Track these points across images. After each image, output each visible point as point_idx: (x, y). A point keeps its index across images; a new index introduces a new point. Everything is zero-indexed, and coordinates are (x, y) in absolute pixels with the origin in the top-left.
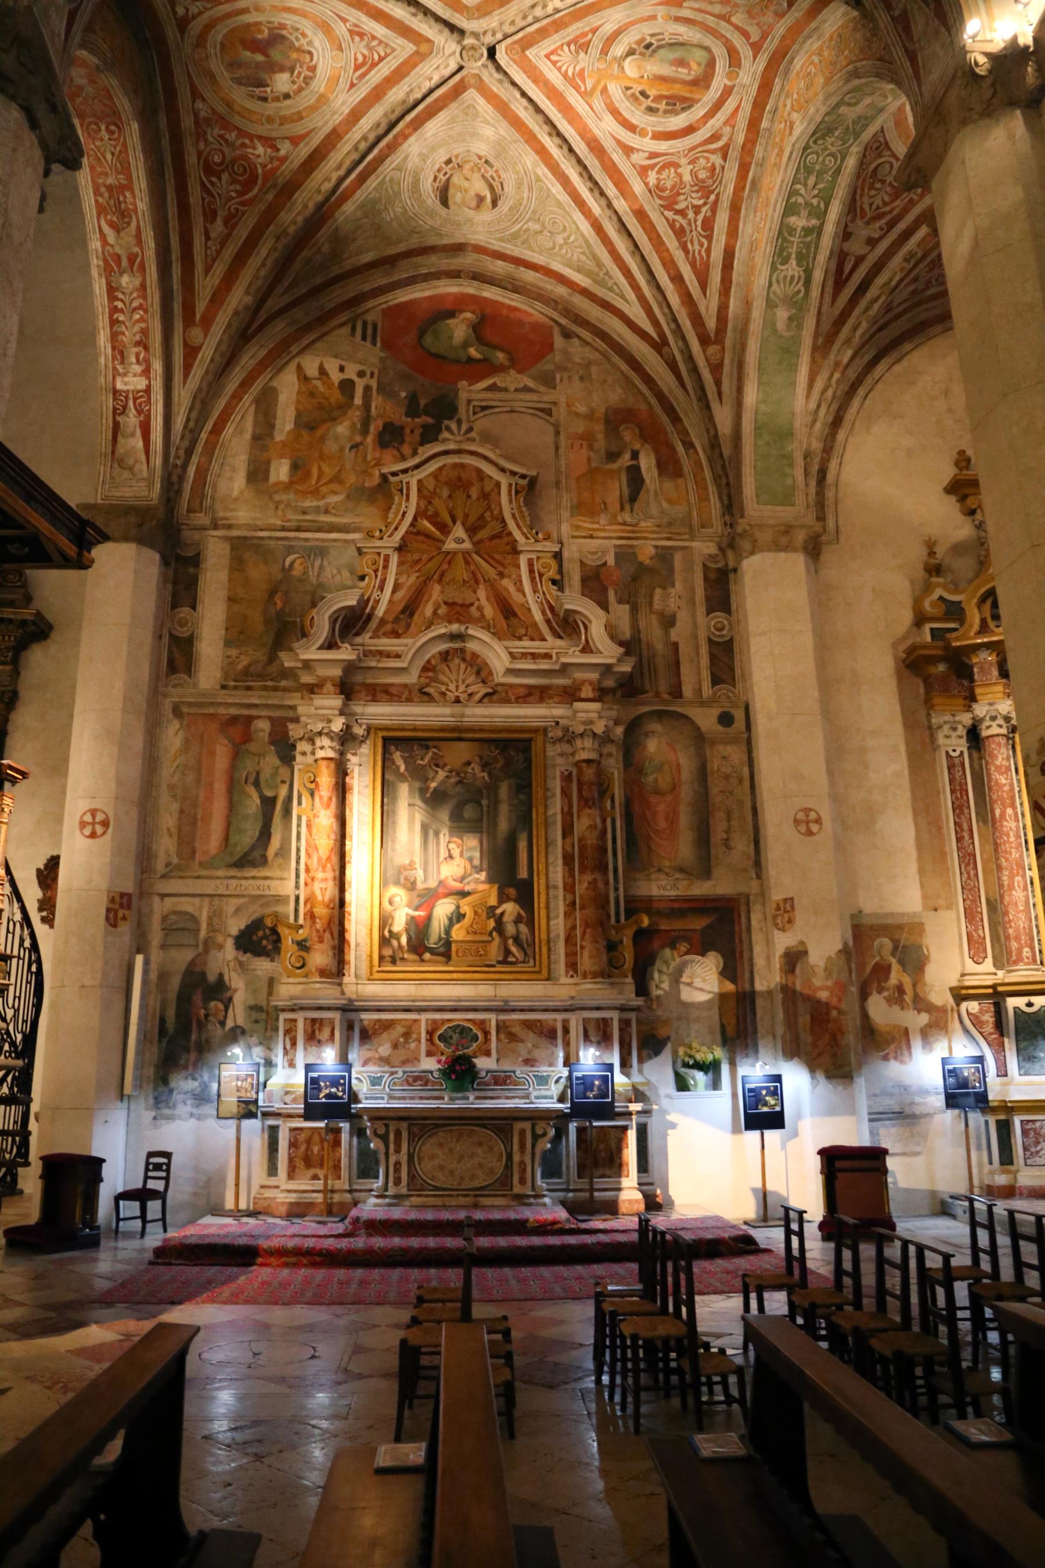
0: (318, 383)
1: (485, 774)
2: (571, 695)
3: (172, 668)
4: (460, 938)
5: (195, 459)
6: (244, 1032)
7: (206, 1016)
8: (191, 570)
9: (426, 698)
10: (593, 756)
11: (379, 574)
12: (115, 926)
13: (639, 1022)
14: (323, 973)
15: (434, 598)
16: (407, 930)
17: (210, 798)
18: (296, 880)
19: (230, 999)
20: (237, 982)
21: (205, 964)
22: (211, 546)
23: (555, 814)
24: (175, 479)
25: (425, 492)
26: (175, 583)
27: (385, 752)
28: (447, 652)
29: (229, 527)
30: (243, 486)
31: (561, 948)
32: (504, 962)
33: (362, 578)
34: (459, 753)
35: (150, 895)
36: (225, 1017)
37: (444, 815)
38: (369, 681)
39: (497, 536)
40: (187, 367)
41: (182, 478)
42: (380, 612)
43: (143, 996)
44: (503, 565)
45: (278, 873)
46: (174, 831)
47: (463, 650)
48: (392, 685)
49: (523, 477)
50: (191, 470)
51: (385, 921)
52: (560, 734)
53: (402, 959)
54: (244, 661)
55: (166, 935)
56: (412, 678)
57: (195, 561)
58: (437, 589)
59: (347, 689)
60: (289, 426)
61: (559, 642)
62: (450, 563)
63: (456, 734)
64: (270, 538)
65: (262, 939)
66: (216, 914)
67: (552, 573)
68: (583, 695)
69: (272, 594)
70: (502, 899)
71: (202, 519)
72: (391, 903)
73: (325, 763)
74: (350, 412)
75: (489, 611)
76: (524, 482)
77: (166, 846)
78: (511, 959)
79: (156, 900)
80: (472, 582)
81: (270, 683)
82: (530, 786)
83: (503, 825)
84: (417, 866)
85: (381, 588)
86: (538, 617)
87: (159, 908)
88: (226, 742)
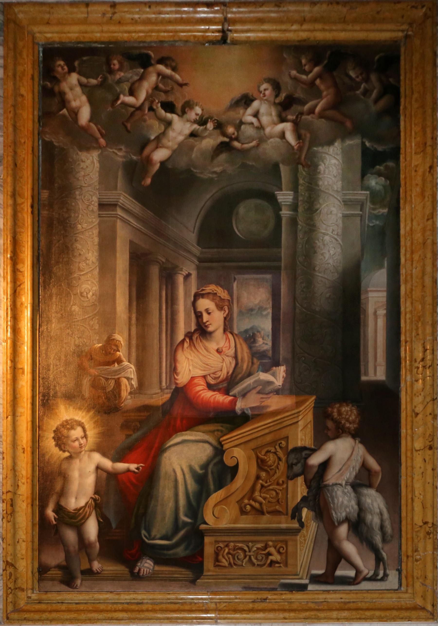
4: (224, 524)
16: (98, 505)
32: (328, 578)
53: (89, 573)
78: (343, 571)
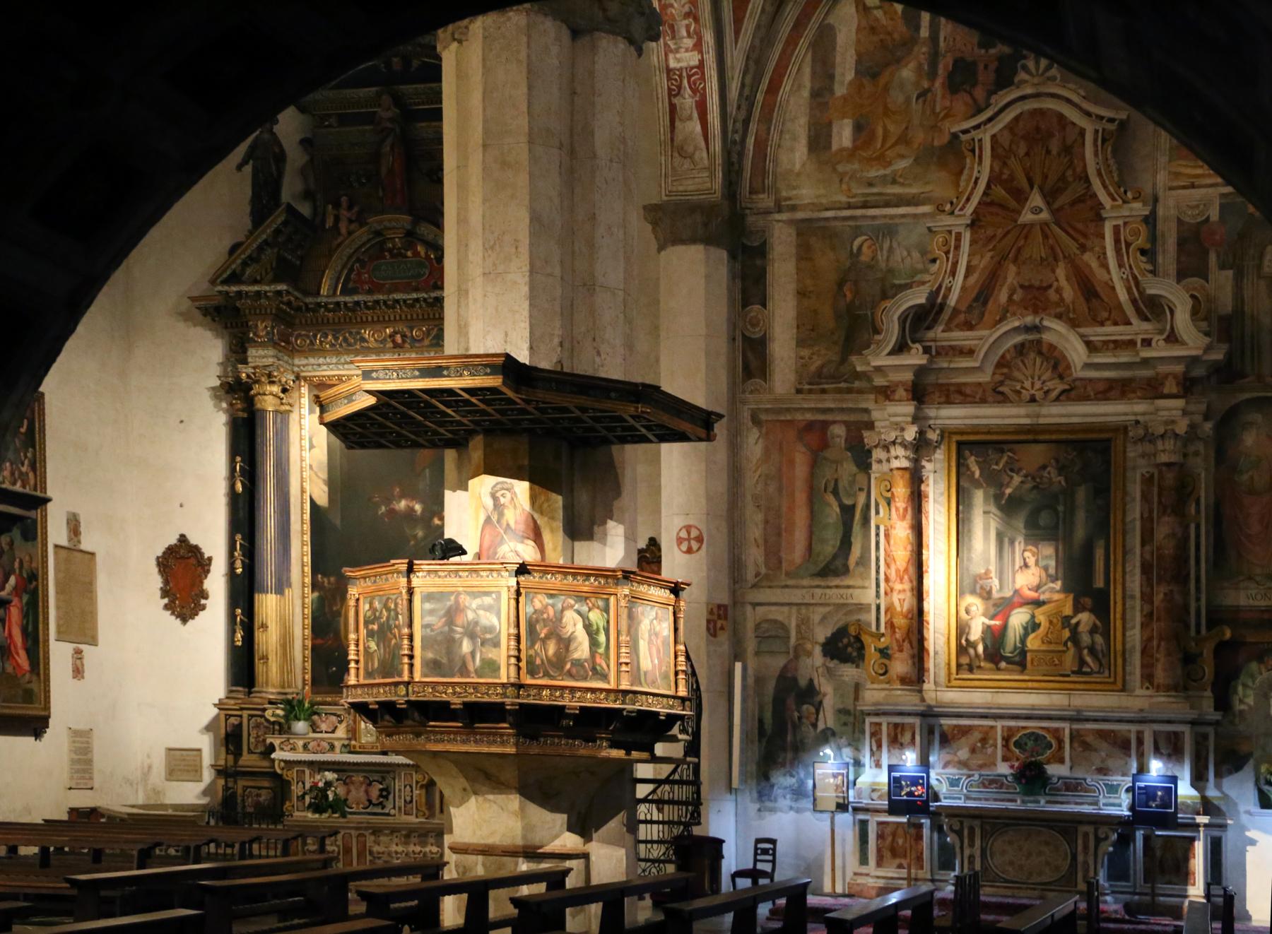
0: (878, 14)
1: (1061, 479)
2: (1153, 389)
3: (748, 373)
4: (1035, 648)
5: (753, 127)
6: (834, 734)
7: (800, 718)
8: (758, 262)
9: (1000, 398)
10: (1174, 458)
11: (951, 256)
12: (715, 635)
13: (1216, 734)
14: (904, 680)
15: (1009, 280)
16: (983, 639)
17: (791, 509)
18: (877, 590)
19: (821, 703)
20: (826, 687)
21: (796, 670)
22: (776, 233)
23: (1134, 519)
24: (735, 158)
25: (1000, 150)
26: (744, 278)
27: (960, 456)
28: (1022, 345)
29: (793, 208)
30: (805, 158)
31: (1136, 659)
32: (1079, 672)
33: (934, 261)
34: (1035, 455)
35: (743, 604)
36: (817, 719)
37: (1020, 523)
38: (940, 381)
39: (1080, 200)
40: (738, 22)
41: (741, 154)
42: (952, 300)
43: (744, 700)
44: (1085, 236)
45: (859, 582)
46: (761, 541)
47: (1039, 342)
48: (965, 384)
49: (1111, 120)
50: (750, 141)
51: (962, 629)
52: (1141, 432)
53: (979, 667)
54: (818, 362)
55: (760, 643)
56: (985, 377)
57: (761, 251)
58: (1012, 269)
59: (919, 392)
60: (850, 76)
61: (1146, 326)
62: (1026, 238)
63: (1032, 434)
64: (835, 218)
65: (846, 646)
66: (804, 622)
67: (1141, 242)
68: (1166, 391)
69: (840, 284)
70: (1078, 608)
71: (765, 201)
72: (967, 612)
73: (900, 472)
74: (916, 49)
75: (1069, 293)
76: (1112, 127)
77: (754, 557)
78: (1086, 669)
79: (749, 608)
80: (1051, 259)
81: (843, 385)
82: (1108, 489)
83: (1080, 533)
84: (993, 575)
85: (953, 273)
86: (1123, 295)
87: (751, 617)
88: (803, 449)
